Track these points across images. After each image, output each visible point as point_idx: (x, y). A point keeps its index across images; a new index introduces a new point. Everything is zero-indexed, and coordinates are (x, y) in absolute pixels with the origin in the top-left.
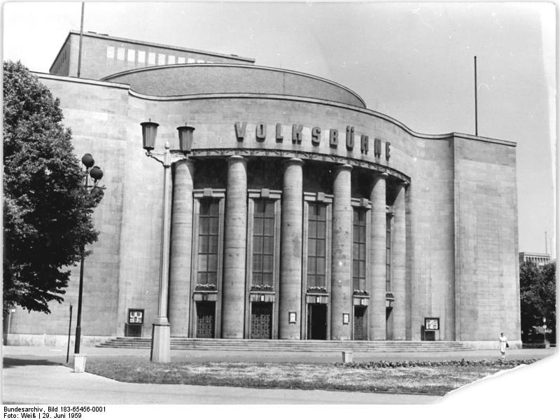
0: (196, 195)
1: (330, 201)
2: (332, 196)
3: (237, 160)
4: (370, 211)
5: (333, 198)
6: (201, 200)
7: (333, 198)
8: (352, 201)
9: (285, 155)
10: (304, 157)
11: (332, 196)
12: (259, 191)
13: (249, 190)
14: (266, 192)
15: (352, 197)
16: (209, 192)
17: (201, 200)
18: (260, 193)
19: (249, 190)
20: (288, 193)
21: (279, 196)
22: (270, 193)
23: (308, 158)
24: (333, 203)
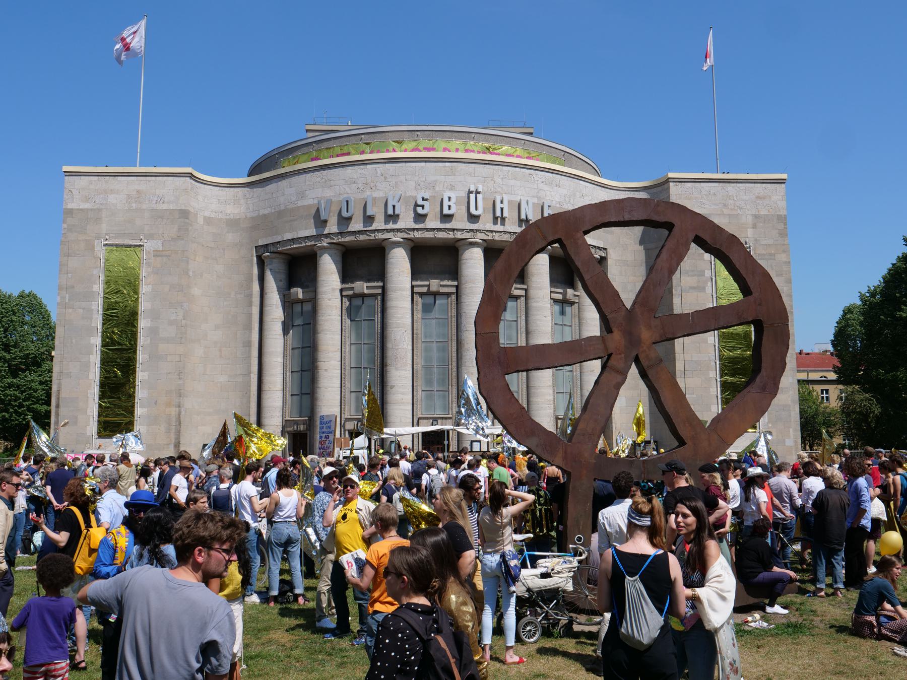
0: (344, 293)
1: (523, 293)
2: (525, 287)
3: (396, 244)
4: (576, 305)
5: (526, 290)
6: (350, 298)
7: (526, 290)
8: (551, 292)
9: (459, 235)
10: (485, 237)
11: (525, 287)
12: (427, 283)
13: (415, 283)
14: (434, 284)
15: (551, 286)
16: (362, 287)
17: (350, 298)
18: (428, 286)
19: (415, 283)
20: (463, 282)
21: (454, 290)
22: (441, 286)
23: (490, 238)
24: (526, 297)
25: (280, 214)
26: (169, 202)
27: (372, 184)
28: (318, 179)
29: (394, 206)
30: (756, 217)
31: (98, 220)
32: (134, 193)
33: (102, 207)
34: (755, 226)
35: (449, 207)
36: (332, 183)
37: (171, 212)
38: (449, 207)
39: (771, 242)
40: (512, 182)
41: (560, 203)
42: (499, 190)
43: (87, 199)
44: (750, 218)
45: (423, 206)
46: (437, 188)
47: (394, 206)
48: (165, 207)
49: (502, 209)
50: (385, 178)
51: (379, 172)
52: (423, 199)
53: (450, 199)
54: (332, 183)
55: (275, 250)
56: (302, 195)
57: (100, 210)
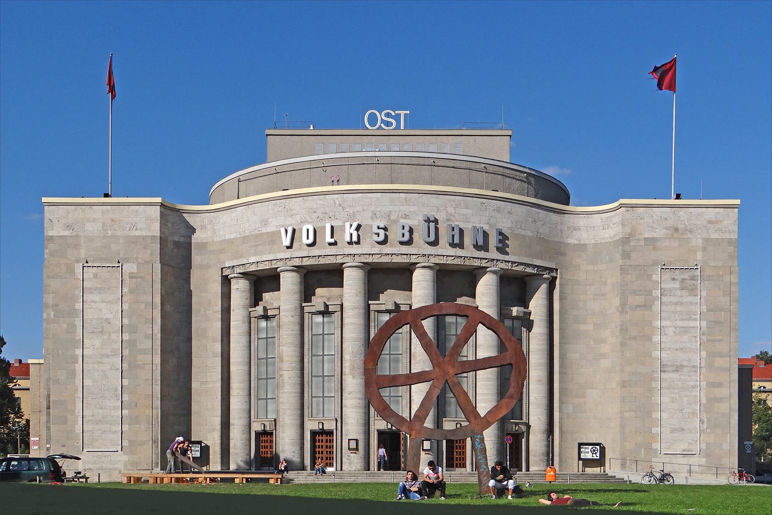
9: (413, 259)
25: (245, 239)
26: (141, 230)
27: (331, 214)
28: (280, 209)
29: (351, 235)
30: (706, 240)
31: (77, 246)
32: (110, 221)
33: (80, 234)
34: (704, 249)
35: (403, 235)
36: (293, 212)
37: (144, 238)
38: (403, 235)
39: (720, 264)
40: (464, 211)
41: (510, 228)
42: (452, 218)
43: (68, 227)
44: (700, 242)
45: (378, 235)
46: (392, 218)
47: (351, 235)
48: (138, 233)
49: (453, 236)
50: (343, 208)
51: (338, 203)
52: (379, 228)
53: (403, 228)
54: (293, 212)
55: (241, 271)
56: (265, 223)
57: (77, 236)
